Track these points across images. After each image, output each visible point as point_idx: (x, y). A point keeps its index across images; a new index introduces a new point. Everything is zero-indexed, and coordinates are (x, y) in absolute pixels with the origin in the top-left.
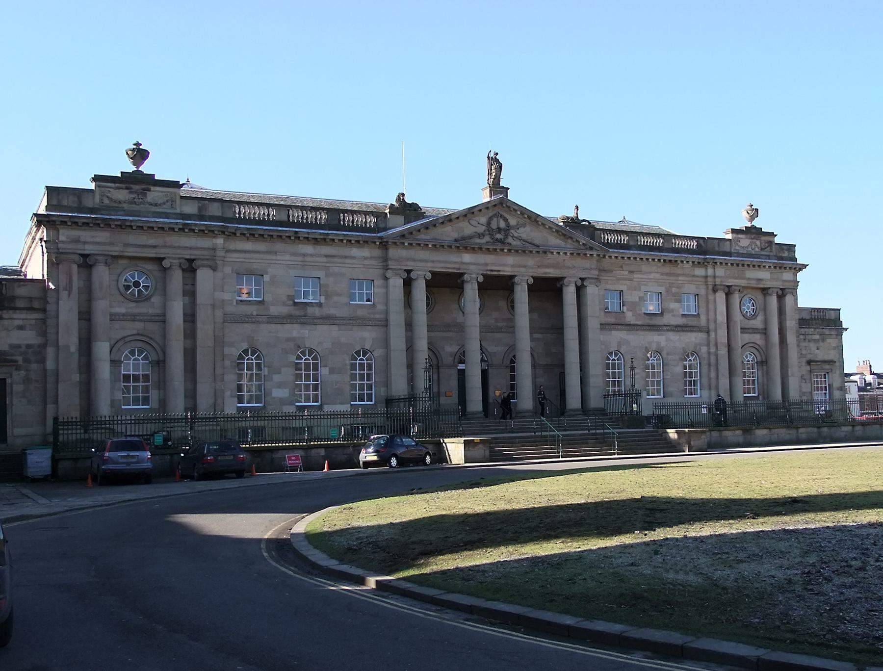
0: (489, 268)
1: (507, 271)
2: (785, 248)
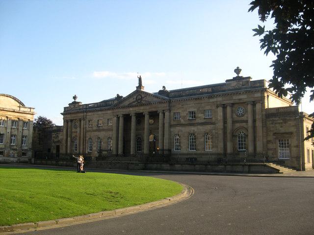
1: (141, 111)
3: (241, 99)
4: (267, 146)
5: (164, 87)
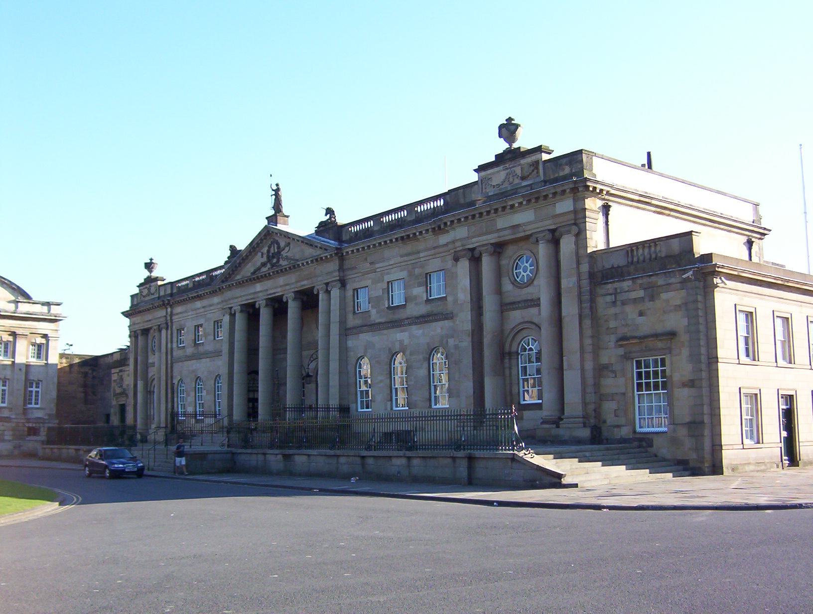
2: (564, 161)
3: (518, 226)
4: (597, 385)
5: (330, 211)
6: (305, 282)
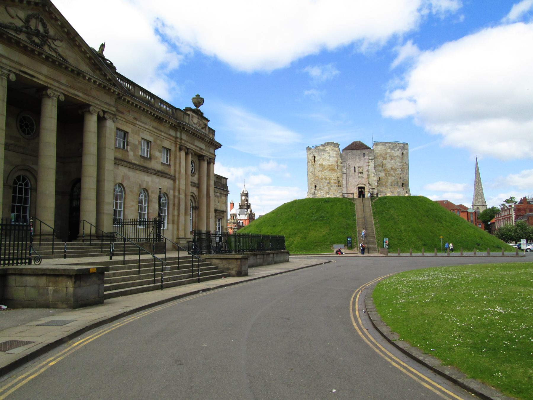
0: (23, 69)
1: (42, 80)
5: (103, 46)
6: (81, 94)
